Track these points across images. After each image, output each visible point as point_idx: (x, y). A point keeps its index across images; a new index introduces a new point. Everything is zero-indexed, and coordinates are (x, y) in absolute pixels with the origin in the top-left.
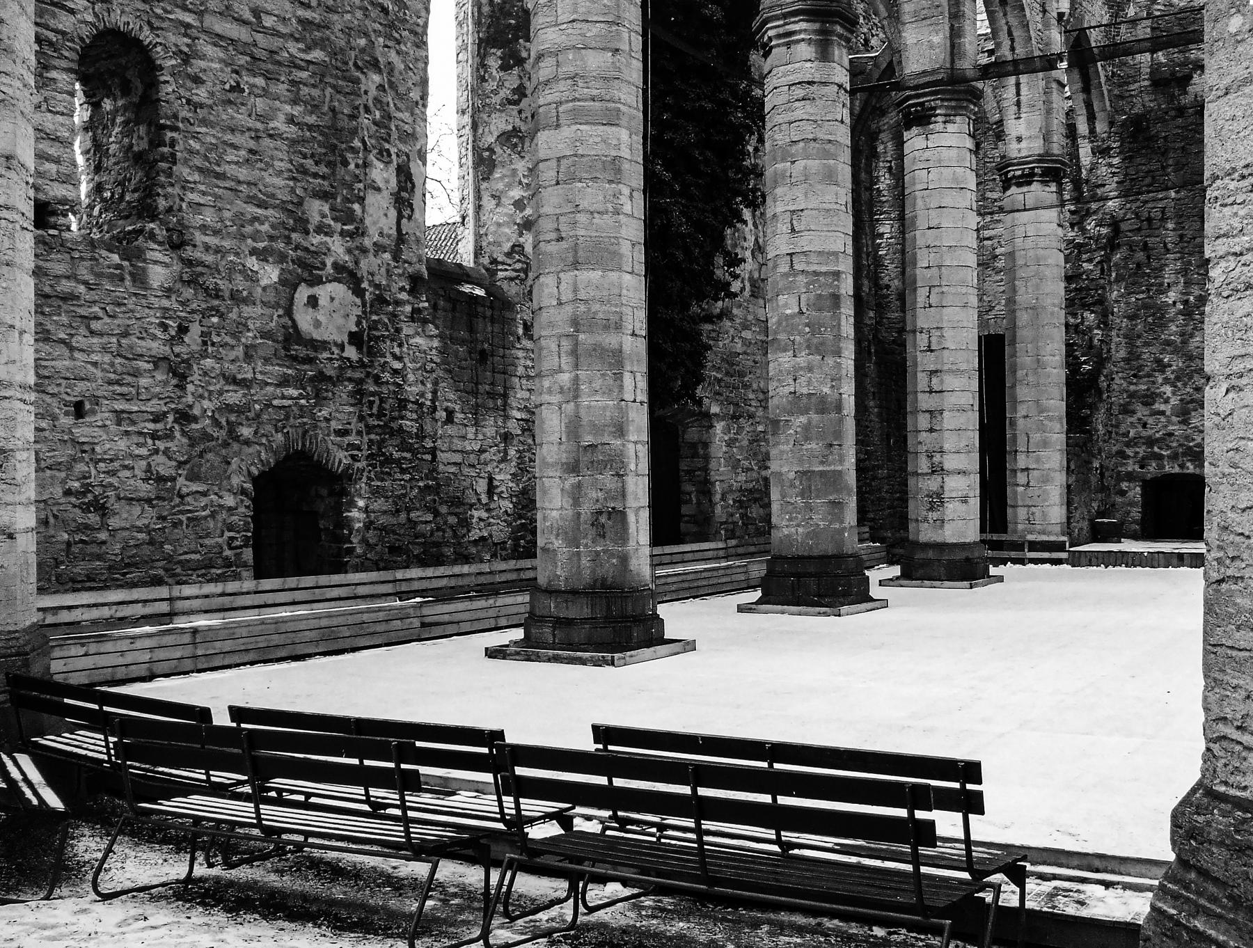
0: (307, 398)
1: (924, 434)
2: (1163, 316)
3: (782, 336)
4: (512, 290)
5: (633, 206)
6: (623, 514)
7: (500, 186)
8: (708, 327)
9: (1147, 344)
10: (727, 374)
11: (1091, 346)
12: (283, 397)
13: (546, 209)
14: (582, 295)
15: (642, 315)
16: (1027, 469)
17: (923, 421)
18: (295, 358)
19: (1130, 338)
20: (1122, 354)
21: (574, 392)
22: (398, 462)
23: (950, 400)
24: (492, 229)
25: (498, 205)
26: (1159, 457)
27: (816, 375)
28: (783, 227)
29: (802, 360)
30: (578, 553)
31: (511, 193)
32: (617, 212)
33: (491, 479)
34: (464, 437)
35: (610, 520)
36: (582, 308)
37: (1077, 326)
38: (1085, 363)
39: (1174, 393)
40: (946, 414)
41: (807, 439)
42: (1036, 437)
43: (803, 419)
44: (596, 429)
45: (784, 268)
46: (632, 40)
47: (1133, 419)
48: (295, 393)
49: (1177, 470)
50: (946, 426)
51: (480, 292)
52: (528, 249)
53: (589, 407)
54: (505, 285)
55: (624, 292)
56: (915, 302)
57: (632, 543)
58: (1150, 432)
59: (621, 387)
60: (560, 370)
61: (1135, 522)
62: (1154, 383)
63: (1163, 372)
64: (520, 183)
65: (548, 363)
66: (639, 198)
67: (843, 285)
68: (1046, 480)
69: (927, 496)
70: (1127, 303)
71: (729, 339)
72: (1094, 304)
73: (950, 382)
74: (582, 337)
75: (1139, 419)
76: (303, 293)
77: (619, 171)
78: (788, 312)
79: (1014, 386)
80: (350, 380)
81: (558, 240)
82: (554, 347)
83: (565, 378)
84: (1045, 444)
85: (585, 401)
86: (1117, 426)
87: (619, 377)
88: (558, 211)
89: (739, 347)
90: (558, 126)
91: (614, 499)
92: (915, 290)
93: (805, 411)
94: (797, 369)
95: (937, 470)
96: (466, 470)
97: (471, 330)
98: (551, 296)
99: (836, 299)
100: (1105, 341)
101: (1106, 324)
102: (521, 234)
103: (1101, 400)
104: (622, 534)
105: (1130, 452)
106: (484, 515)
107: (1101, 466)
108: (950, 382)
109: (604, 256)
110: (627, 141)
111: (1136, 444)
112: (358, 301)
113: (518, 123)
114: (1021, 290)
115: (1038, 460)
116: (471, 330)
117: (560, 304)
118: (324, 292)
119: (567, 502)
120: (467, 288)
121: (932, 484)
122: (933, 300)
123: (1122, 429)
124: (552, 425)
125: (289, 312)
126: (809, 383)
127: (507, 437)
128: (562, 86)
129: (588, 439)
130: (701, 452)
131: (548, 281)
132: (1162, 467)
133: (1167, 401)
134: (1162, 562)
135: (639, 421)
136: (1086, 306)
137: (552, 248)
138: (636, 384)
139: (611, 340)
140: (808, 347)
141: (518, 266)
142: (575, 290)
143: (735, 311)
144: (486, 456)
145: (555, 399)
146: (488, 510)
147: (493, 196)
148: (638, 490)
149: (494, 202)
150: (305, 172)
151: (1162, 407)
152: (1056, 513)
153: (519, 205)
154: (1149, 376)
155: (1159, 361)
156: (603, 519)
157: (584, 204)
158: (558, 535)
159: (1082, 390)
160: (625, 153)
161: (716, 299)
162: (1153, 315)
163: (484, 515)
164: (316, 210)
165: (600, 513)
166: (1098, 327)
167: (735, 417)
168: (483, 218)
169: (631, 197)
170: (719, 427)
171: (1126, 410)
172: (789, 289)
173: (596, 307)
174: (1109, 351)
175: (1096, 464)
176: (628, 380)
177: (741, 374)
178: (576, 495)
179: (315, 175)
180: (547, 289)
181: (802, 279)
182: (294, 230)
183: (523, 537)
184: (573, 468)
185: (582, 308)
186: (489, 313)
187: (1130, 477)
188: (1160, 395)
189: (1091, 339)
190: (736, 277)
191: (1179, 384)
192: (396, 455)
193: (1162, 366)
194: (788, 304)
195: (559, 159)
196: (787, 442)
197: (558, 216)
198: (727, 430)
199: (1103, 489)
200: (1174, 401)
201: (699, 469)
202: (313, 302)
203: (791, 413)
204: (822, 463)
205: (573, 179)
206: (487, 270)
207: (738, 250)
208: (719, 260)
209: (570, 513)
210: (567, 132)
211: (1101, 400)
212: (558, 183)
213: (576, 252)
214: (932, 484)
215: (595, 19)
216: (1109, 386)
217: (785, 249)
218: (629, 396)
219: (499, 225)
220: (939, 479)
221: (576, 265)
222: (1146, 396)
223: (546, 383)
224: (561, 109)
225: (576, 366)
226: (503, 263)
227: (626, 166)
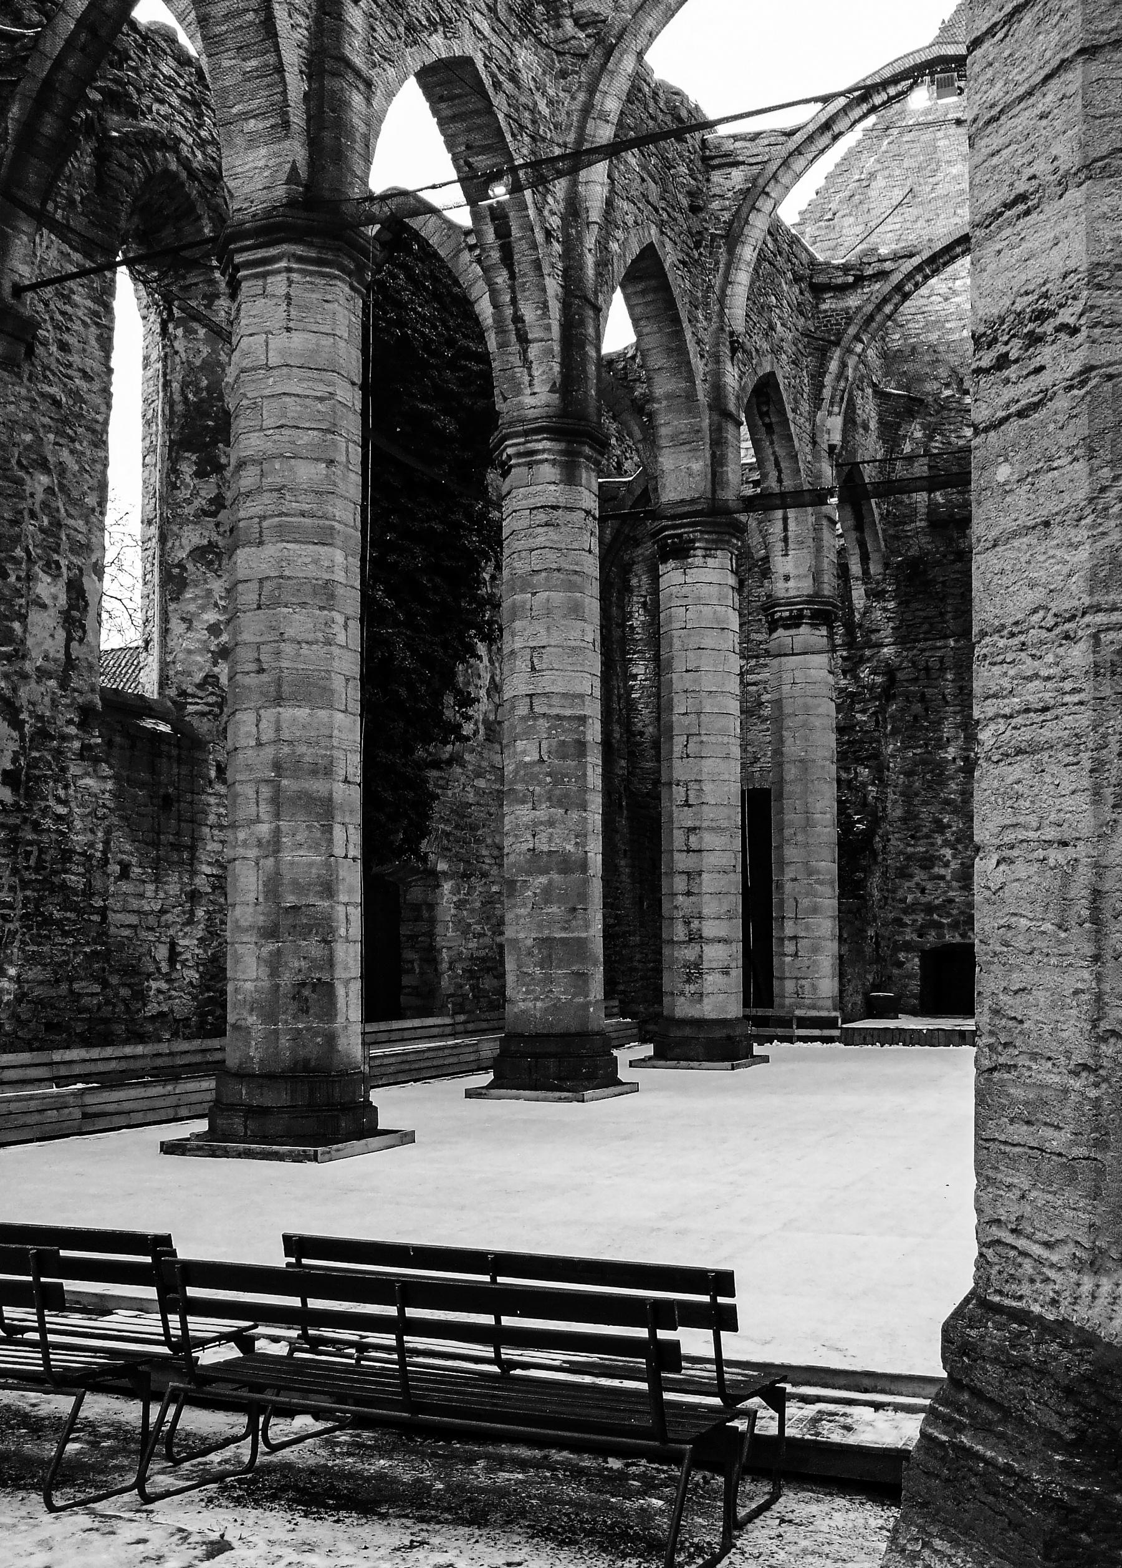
1: (680, 898)
2: (942, 774)
3: (519, 787)
4: (203, 726)
5: (348, 635)
6: (330, 986)
7: (192, 608)
8: (434, 773)
9: (925, 803)
10: (457, 827)
11: (865, 803)
13: (246, 637)
14: (286, 735)
15: (356, 759)
16: (795, 938)
17: (680, 884)
19: (908, 795)
20: (899, 813)
21: (274, 845)
23: (710, 860)
24: (181, 656)
25: (188, 629)
26: (939, 926)
27: (557, 831)
28: (522, 664)
29: (542, 814)
30: (276, 1031)
31: (205, 617)
32: (328, 643)
33: (173, 945)
34: (141, 896)
35: (316, 994)
36: (286, 750)
37: (850, 781)
38: (859, 821)
39: (954, 856)
40: (704, 875)
41: (547, 902)
42: (805, 902)
43: (543, 880)
44: (299, 888)
45: (522, 710)
46: (349, 451)
47: (912, 884)
49: (958, 939)
50: (704, 890)
51: (165, 728)
52: (224, 680)
53: (292, 863)
54: (196, 722)
55: (336, 732)
56: (671, 752)
57: (340, 1019)
58: (929, 898)
59: (330, 841)
60: (258, 820)
61: (914, 996)
62: (933, 844)
63: (943, 834)
64: (216, 605)
65: (246, 811)
66: (355, 626)
67: (589, 732)
68: (815, 950)
69: (684, 966)
70: (903, 759)
71: (461, 787)
72: (868, 758)
73: (709, 840)
74: (285, 782)
75: (917, 884)
77: (332, 596)
78: (527, 759)
79: (780, 847)
81: (258, 672)
82: (251, 794)
83: (264, 829)
84: (815, 910)
85: (287, 856)
86: (894, 891)
87: (328, 830)
88: (259, 639)
89: (471, 797)
90: (261, 543)
91: (321, 969)
92: (672, 737)
93: (545, 871)
94: (536, 823)
95: (695, 938)
96: (144, 934)
97: (153, 771)
98: (248, 735)
99: (581, 747)
100: (881, 799)
101: (881, 780)
102: (215, 664)
103: (876, 862)
104: (329, 1010)
105: (907, 920)
106: (164, 986)
107: (877, 935)
108: (709, 840)
109: (313, 691)
110: (342, 564)
111: (914, 911)
113: (215, 538)
114: (789, 741)
115: (807, 928)
116: (153, 771)
117: (259, 744)
119: (264, 972)
120: (149, 723)
121: (689, 953)
122: (692, 748)
123: (900, 894)
124: (248, 882)
126: (550, 840)
127: (194, 896)
128: (267, 498)
129: (290, 900)
130: (426, 914)
131: (246, 719)
132: (941, 936)
133: (946, 865)
134: (942, 1040)
135: (351, 881)
136: (859, 761)
137: (251, 680)
138: (348, 838)
139: (318, 786)
140: (549, 799)
141: (212, 699)
142: (278, 730)
143: (467, 757)
144: (169, 918)
145: (252, 853)
146: (169, 981)
147: (183, 619)
148: (349, 958)
149: (184, 626)
151: (942, 871)
152: (828, 986)
153: (214, 630)
154: (927, 836)
155: (938, 821)
156: (306, 992)
157: (290, 632)
158: (252, 1010)
159: (855, 851)
160: (340, 576)
161: (445, 742)
162: (932, 771)
163: (164, 986)
165: (303, 984)
166: (873, 784)
167: (466, 876)
168: (171, 644)
169: (346, 626)
170: (447, 886)
171: (904, 874)
172: (527, 734)
173: (302, 749)
174: (884, 809)
175: (871, 932)
176: (338, 832)
177: (473, 828)
178: (274, 965)
180: (245, 726)
181: (543, 724)
183: (210, 1013)
184: (270, 933)
185: (286, 750)
186: (174, 752)
187: (908, 947)
188: (940, 858)
189: (865, 796)
190: (468, 718)
191: (959, 847)
193: (941, 828)
194: (527, 751)
195: (261, 581)
196: (524, 905)
197: (258, 646)
198: (456, 891)
199: (879, 959)
200: (954, 865)
201: (423, 934)
203: (529, 873)
204: (565, 929)
205: (276, 603)
206: (174, 702)
207: (471, 689)
208: (449, 699)
209: (266, 984)
211: (876, 862)
212: (259, 608)
213: (280, 686)
214: (689, 953)
215: (307, 425)
216: (884, 847)
217: (523, 689)
218: (339, 851)
219: (189, 652)
220: (698, 948)
221: (279, 700)
222: (925, 859)
223: (242, 835)
224: (265, 524)
225: (277, 816)
226: (193, 696)
227: (340, 591)
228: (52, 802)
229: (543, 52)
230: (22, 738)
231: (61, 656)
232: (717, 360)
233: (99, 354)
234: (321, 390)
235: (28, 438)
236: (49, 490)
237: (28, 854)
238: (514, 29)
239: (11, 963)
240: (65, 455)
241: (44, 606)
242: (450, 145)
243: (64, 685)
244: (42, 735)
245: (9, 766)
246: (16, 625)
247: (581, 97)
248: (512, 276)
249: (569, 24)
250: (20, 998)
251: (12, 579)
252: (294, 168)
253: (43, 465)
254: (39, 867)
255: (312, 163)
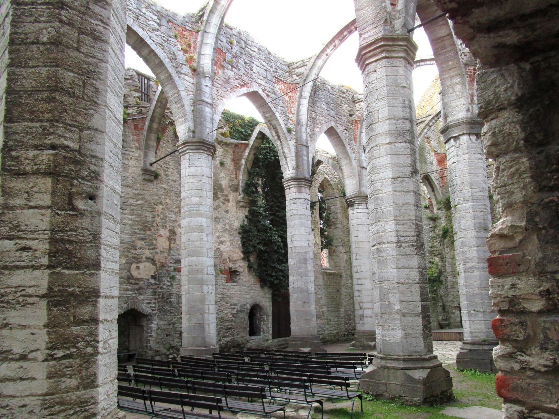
0: (136, 294)
12: (127, 294)
18: (131, 283)
22: (169, 311)
48: (131, 293)
76: (134, 266)
80: (151, 288)
112: (155, 267)
118: (142, 266)
125: (129, 271)
150: (135, 233)
164: (139, 243)
179: (139, 234)
182: (131, 249)
192: (169, 309)
202: (138, 268)
210: (187, 220)
228: (166, 282)
229: (286, 85)
230: (156, 267)
231: (168, 247)
233: (178, 176)
234: (198, 180)
235: (156, 197)
236: (163, 209)
237: (159, 295)
238: (274, 81)
239: (155, 320)
240: (168, 201)
241: (162, 236)
242: (260, 112)
243: (169, 253)
244: (163, 266)
245: (153, 274)
246: (154, 241)
247: (298, 94)
248: (281, 142)
249: (294, 76)
250: (158, 329)
251: (153, 231)
252: (189, 129)
253: (161, 203)
254: (163, 298)
255: (195, 126)
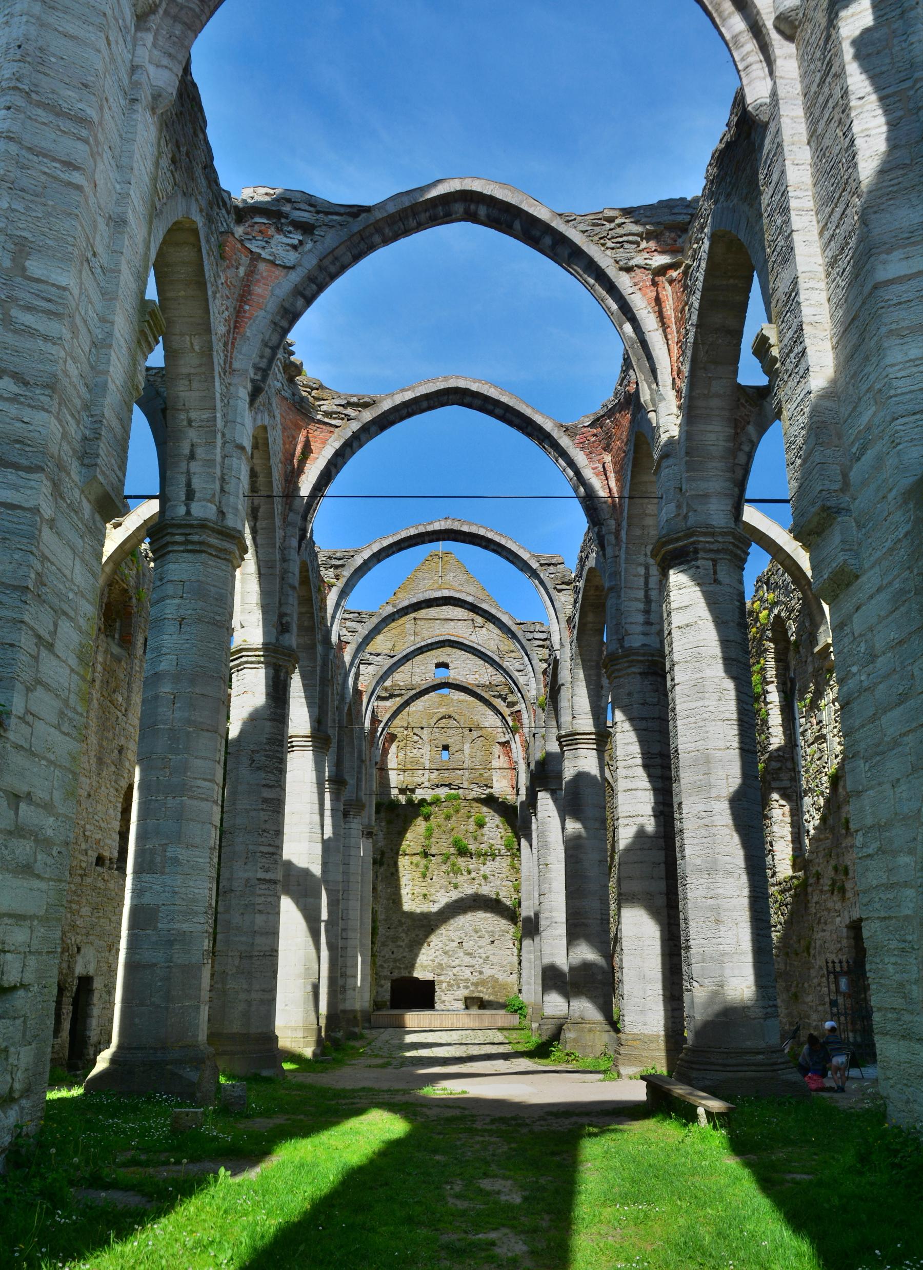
20: (383, 917)
26: (400, 968)
105: (385, 965)
133: (403, 941)
155: (400, 921)
187: (385, 978)
232: (361, 741)
